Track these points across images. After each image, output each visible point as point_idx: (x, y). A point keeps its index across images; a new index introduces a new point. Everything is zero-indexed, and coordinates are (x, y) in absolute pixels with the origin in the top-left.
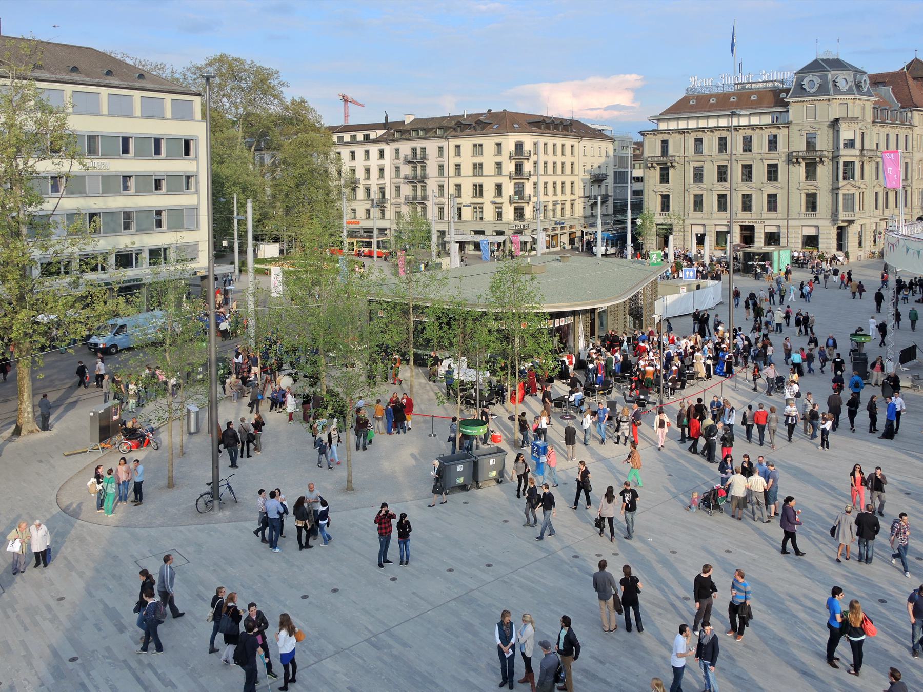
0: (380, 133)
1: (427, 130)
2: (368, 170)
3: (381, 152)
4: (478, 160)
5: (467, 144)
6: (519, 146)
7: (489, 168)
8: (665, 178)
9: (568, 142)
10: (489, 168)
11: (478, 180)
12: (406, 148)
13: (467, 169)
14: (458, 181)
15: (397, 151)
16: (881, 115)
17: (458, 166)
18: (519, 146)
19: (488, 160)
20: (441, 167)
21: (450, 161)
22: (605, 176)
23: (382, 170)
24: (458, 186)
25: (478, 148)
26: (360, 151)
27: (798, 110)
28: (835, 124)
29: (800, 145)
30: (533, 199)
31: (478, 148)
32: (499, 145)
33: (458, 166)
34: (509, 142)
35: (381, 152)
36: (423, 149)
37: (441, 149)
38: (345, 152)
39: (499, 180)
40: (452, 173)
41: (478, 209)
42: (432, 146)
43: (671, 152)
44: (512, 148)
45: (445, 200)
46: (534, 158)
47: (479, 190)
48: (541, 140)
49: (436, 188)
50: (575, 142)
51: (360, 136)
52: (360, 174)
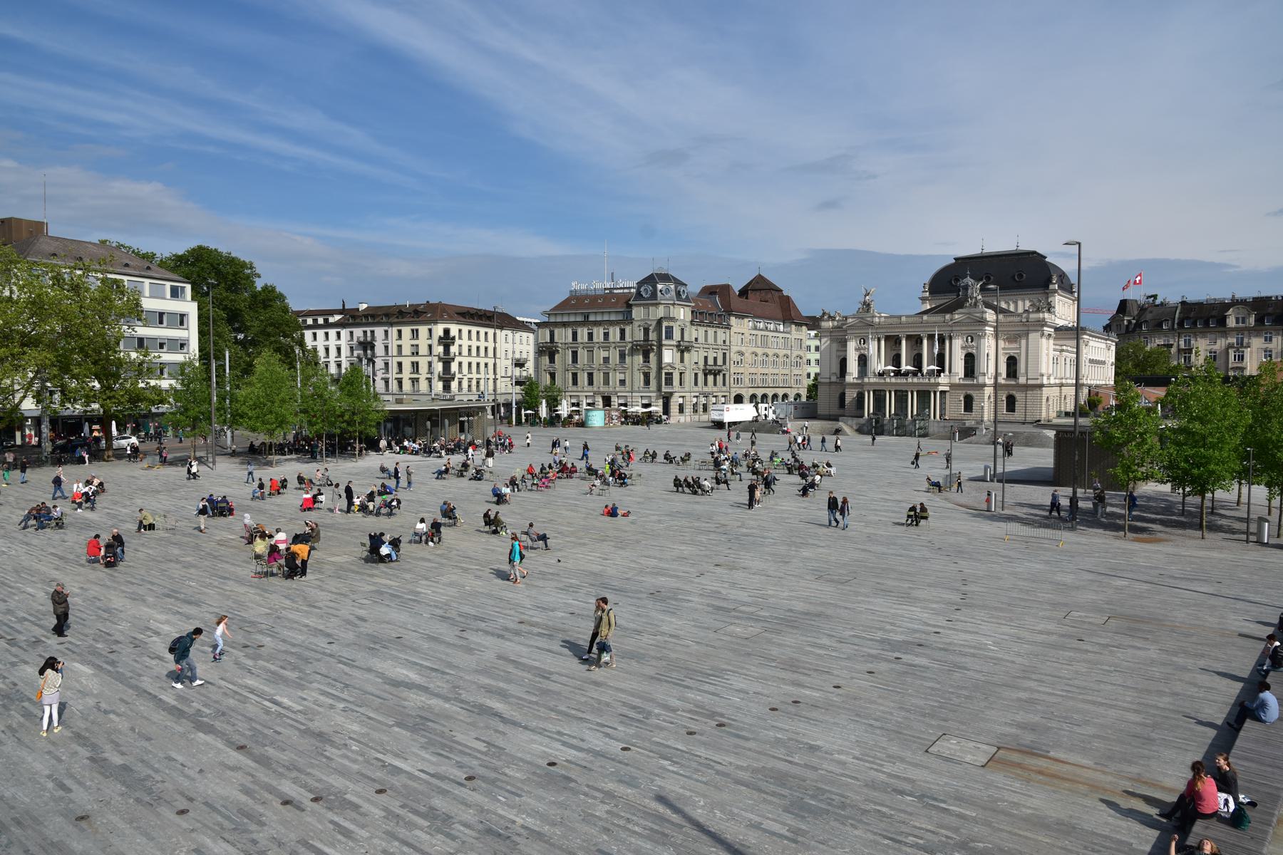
0: (337, 317)
1: (373, 316)
2: (327, 350)
3: (339, 334)
4: (415, 342)
5: (406, 331)
6: (447, 331)
7: (423, 350)
8: (552, 360)
9: (491, 331)
10: (423, 350)
11: (415, 359)
12: (358, 332)
13: (407, 350)
14: (400, 359)
15: (351, 333)
16: (699, 317)
17: (400, 347)
18: (447, 331)
19: (423, 342)
20: (386, 348)
21: (393, 343)
22: (526, 360)
23: (339, 349)
24: (400, 364)
25: (415, 334)
26: (320, 333)
27: (638, 313)
28: (659, 322)
29: (640, 336)
30: (458, 376)
31: (415, 334)
32: (430, 330)
33: (400, 347)
34: (439, 330)
35: (339, 334)
36: (373, 332)
37: (386, 332)
38: (308, 334)
39: (429, 359)
40: (395, 353)
41: (414, 381)
42: (379, 331)
43: (556, 339)
44: (441, 334)
45: (389, 376)
46: (457, 342)
47: (415, 366)
48: (465, 329)
49: (382, 365)
50: (498, 331)
51: (321, 321)
52: (322, 353)
